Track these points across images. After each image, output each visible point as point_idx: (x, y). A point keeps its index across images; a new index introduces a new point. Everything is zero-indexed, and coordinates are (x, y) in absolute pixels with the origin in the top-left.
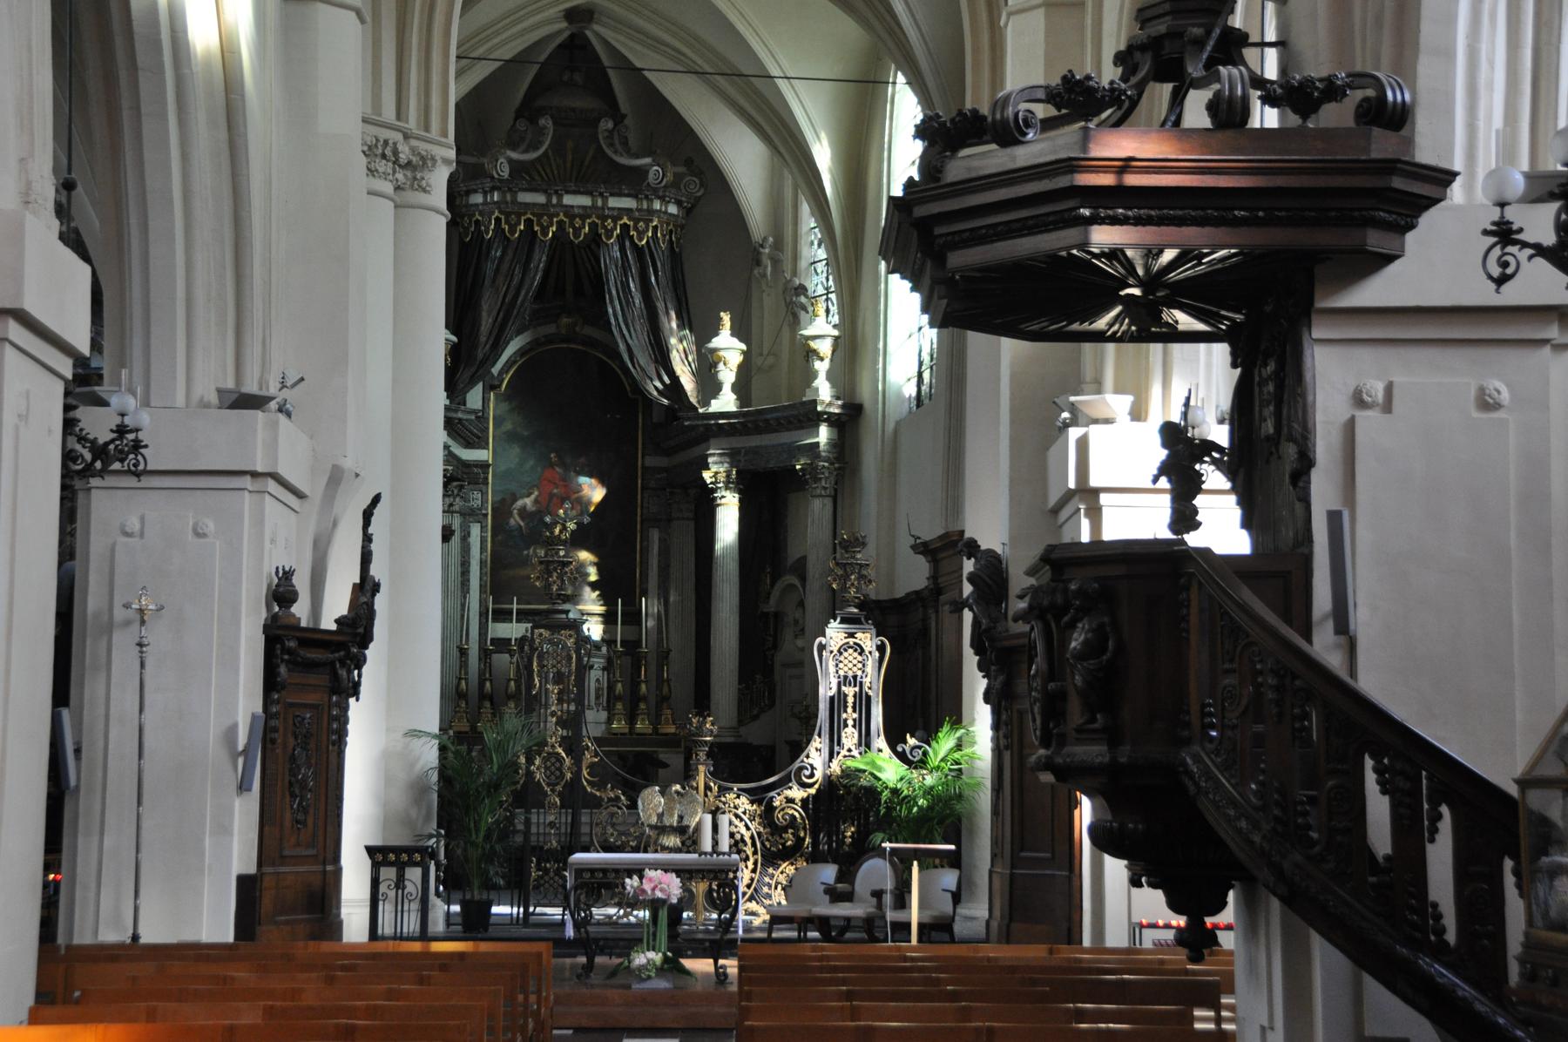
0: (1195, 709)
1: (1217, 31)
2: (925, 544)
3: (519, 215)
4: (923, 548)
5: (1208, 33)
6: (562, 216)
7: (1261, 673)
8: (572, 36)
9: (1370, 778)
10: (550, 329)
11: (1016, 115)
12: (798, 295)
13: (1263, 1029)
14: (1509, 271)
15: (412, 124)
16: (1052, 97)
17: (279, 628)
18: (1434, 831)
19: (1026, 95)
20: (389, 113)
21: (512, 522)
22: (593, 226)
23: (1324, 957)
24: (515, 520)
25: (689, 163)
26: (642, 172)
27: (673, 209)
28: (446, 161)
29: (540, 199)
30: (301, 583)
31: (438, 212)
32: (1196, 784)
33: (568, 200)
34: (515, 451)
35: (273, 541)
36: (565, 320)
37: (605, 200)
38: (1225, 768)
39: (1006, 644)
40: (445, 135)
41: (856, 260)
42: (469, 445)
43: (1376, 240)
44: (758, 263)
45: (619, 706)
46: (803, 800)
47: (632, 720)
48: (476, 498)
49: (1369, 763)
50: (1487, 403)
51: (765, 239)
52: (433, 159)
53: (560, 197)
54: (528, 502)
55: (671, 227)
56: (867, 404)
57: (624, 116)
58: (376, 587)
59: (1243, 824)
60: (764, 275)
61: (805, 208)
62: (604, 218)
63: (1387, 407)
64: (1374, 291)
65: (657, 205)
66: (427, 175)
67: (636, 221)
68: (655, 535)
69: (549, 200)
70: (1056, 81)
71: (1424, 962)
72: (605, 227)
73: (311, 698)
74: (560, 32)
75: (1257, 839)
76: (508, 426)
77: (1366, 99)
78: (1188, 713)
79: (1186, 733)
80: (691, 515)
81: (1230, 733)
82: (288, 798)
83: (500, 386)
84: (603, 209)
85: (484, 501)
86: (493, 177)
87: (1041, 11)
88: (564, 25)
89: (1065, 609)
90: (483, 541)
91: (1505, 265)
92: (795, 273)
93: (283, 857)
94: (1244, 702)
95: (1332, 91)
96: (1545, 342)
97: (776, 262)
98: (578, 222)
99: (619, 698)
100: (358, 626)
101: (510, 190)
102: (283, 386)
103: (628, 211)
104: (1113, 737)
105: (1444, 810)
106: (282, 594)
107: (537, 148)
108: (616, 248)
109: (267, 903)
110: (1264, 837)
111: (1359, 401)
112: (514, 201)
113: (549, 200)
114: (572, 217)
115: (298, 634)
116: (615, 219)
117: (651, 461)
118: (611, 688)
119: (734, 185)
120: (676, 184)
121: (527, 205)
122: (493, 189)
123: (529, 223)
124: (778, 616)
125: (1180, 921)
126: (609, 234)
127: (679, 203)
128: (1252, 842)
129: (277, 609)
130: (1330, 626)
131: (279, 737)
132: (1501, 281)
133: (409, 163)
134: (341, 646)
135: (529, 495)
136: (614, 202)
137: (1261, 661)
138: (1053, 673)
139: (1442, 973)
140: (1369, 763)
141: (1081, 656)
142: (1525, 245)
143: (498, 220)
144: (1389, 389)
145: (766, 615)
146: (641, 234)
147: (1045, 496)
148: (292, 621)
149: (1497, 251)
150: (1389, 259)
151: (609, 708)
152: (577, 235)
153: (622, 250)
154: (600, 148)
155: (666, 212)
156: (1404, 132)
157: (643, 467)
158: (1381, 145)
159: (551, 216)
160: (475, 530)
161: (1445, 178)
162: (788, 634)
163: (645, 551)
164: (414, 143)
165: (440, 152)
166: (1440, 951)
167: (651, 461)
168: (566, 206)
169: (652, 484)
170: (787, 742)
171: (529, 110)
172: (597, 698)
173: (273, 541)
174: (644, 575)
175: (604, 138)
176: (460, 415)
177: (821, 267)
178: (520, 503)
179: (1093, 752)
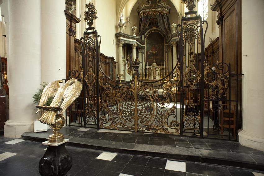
10: (152, 29)
24: (149, 53)
27: (167, 10)
29: (149, 10)
33: (152, 10)
34: (148, 45)
42: (142, 44)
44: (179, 15)
45: (161, 76)
48: (143, 51)
54: (150, 51)
60: (179, 17)
65: (164, 9)
68: (166, 54)
76: (148, 42)
90: (145, 56)
98: (154, 13)
108: (159, 16)
114: (153, 12)
116: (158, 12)
117: (165, 45)
121: (147, 11)
123: (147, 13)
126: (158, 13)
127: (167, 9)
136: (158, 9)
151: (160, 76)
152: (154, 14)
160: (144, 55)
163: (165, 56)
167: (165, 45)
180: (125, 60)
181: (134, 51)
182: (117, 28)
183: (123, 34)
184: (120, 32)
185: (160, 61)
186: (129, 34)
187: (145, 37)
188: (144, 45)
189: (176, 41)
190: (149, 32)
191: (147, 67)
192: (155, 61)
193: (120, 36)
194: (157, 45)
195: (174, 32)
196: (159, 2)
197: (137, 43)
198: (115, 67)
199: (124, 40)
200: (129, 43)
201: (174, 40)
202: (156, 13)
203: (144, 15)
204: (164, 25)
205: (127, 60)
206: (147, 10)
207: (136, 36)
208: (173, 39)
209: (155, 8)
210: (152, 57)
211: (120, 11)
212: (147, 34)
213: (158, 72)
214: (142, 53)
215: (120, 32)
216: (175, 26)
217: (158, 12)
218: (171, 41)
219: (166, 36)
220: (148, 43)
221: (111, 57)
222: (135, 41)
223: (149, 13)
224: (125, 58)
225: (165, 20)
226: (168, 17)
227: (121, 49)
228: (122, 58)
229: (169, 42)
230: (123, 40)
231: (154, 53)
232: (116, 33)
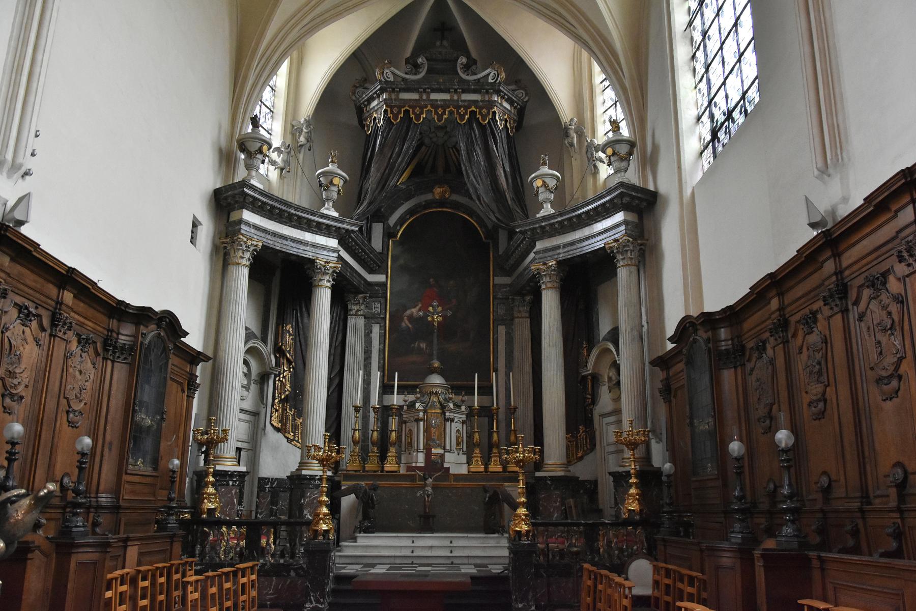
3: (400, 107)
6: (429, 108)
10: (429, 197)
12: (597, 152)
21: (403, 324)
24: (406, 323)
27: (507, 106)
36: (438, 190)
37: (459, 97)
41: (643, 96)
42: (371, 271)
45: (477, 451)
48: (377, 308)
51: (572, 120)
53: (428, 96)
54: (414, 310)
55: (506, 117)
56: (664, 184)
60: (572, 145)
62: (458, 107)
67: (481, 108)
68: (502, 330)
69: (421, 97)
72: (458, 113)
76: (401, 261)
80: (527, 315)
83: (396, 236)
84: (457, 101)
86: (380, 81)
90: (382, 337)
97: (581, 134)
98: (440, 111)
99: (478, 445)
103: (475, 102)
107: (415, 74)
112: (397, 99)
113: (421, 97)
116: (466, 108)
118: (470, 436)
123: (407, 112)
126: (462, 118)
127: (511, 102)
135: (415, 307)
143: (386, 111)
145: (584, 378)
152: (440, 119)
155: (502, 105)
157: (494, 285)
159: (422, 108)
160: (376, 329)
167: (500, 280)
168: (432, 100)
169: (500, 296)
170: (610, 473)
172: (458, 444)
175: (461, 69)
178: (408, 312)
180: (266, 349)
181: (323, 298)
182: (226, 159)
183: (262, 193)
184: (244, 183)
186: (305, 204)
187: (389, 234)
188: (380, 278)
189: (561, 257)
190: (411, 212)
191: (396, 399)
192: (436, 364)
193: (243, 207)
194: (452, 282)
195: (548, 210)
196: (467, 68)
197: (340, 258)
198: (192, 386)
199: (265, 231)
200: (293, 249)
201: (546, 250)
202: (451, 113)
203: (387, 120)
205: (279, 351)
206: (405, 96)
207: (336, 214)
208: (539, 246)
210: (423, 345)
211: (259, 76)
212: (401, 221)
213: (455, 428)
214: (370, 319)
215: (244, 183)
216: (552, 183)
217: (462, 110)
218: (532, 255)
219: (503, 236)
220: (400, 270)
221: (157, 309)
222: (333, 243)
223: (417, 110)
224: (264, 340)
225: (500, 151)
226: (511, 142)
227: (241, 277)
228: (241, 336)
229: (521, 268)
230: (256, 227)
231: (437, 319)
232: (218, 186)
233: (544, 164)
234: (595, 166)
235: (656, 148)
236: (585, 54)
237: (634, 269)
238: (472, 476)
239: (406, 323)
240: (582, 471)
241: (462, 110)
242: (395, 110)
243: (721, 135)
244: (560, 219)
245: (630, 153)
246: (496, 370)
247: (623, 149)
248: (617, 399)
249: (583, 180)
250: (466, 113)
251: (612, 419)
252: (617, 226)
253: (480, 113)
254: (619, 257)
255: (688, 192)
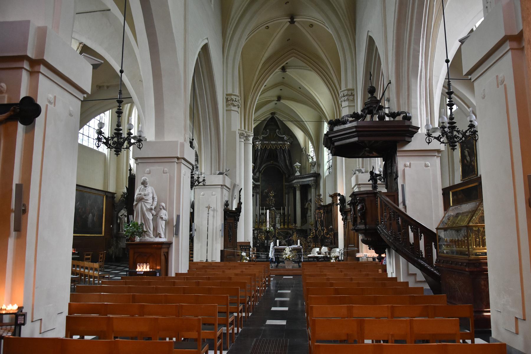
0: (379, 218)
1: (378, 106)
2: (331, 195)
3: (264, 145)
4: (331, 196)
5: (377, 106)
7: (390, 212)
8: (272, 117)
9: (410, 230)
10: (269, 163)
11: (345, 119)
12: (309, 156)
13: (392, 273)
14: (430, 141)
15: (247, 130)
16: (352, 116)
17: (226, 210)
18: (421, 238)
19: (347, 116)
20: (243, 129)
21: (264, 194)
22: (276, 146)
23: (402, 260)
24: (264, 194)
25: (291, 136)
26: (284, 138)
27: (288, 143)
28: (252, 136)
29: (267, 142)
30: (229, 203)
31: (252, 144)
32: (380, 232)
33: (272, 142)
35: (225, 196)
36: (272, 162)
38: (385, 229)
39: (346, 210)
40: (252, 132)
42: (256, 182)
43: (407, 139)
44: (302, 151)
46: (312, 238)
47: (284, 225)
48: (258, 190)
49: (409, 227)
50: (426, 166)
51: (303, 148)
52: (250, 136)
53: (270, 142)
54: (266, 191)
56: (321, 174)
57: (280, 129)
58: (242, 203)
59: (388, 238)
61: (310, 143)
63: (410, 166)
64: (408, 147)
66: (249, 138)
67: (283, 145)
68: (287, 195)
70: (352, 113)
71: (419, 260)
72: (278, 146)
73: (232, 221)
74: (270, 116)
75: (391, 241)
77: (404, 116)
78: (378, 220)
79: (378, 223)
80: (292, 192)
81: (385, 223)
82: (228, 238)
85: (259, 191)
86: (260, 139)
87: (348, 107)
88: (271, 115)
89: (357, 202)
91: (430, 140)
92: (308, 153)
93: (227, 247)
94: (388, 217)
95: (398, 114)
96: (436, 155)
97: (305, 151)
98: (273, 146)
99: (282, 222)
100: (239, 209)
101: (262, 141)
102: (226, 171)
103: (281, 144)
104: (365, 224)
105: (422, 234)
106: (227, 204)
107: (266, 134)
108: (280, 150)
109: (225, 254)
110: (392, 240)
111: (405, 166)
112: (263, 143)
115: (229, 211)
118: (280, 221)
119: (298, 139)
120: (289, 139)
121: (265, 144)
122: (260, 141)
123: (265, 146)
124: (307, 208)
125: (378, 255)
126: (278, 148)
128: (390, 241)
129: (226, 207)
130: (402, 204)
131: (226, 228)
132: (429, 143)
133: (246, 136)
134: (236, 213)
135: (266, 190)
136: (279, 142)
137: (390, 210)
138: (355, 213)
139: (423, 263)
140: (409, 227)
141: (359, 210)
142: (433, 137)
144: (410, 164)
146: (283, 148)
147: (351, 186)
148: (228, 209)
149: (428, 138)
150: (409, 142)
152: (273, 147)
153: (280, 149)
154: (277, 134)
156: (410, 121)
158: (407, 123)
159: (269, 145)
160: (258, 196)
161: (418, 128)
162: (309, 211)
163: (285, 198)
164: (247, 133)
165: (251, 134)
166: (422, 259)
171: (265, 128)
172: (278, 222)
173: (225, 196)
174: (285, 202)
176: (255, 177)
177: (313, 152)
178: (265, 191)
179: (362, 227)
185: (279, 205)
187: (260, 172)
189: (301, 184)
190: (265, 167)
203: (261, 148)
204: (286, 163)
209: (275, 141)
216: (299, 167)
217: (278, 146)
223: (268, 146)
233: (297, 162)
234: (309, 160)
235: (320, 164)
236: (307, 138)
237: (315, 189)
238: (281, 229)
239: (264, 194)
240: (304, 228)
241: (278, 146)
242: (263, 146)
243: (330, 168)
244: (300, 176)
245: (315, 165)
246: (285, 205)
247: (314, 164)
248: (311, 214)
249: (306, 164)
250: (279, 146)
251: (310, 217)
252: (312, 180)
253: (283, 146)
254: (312, 187)
255: (325, 177)
